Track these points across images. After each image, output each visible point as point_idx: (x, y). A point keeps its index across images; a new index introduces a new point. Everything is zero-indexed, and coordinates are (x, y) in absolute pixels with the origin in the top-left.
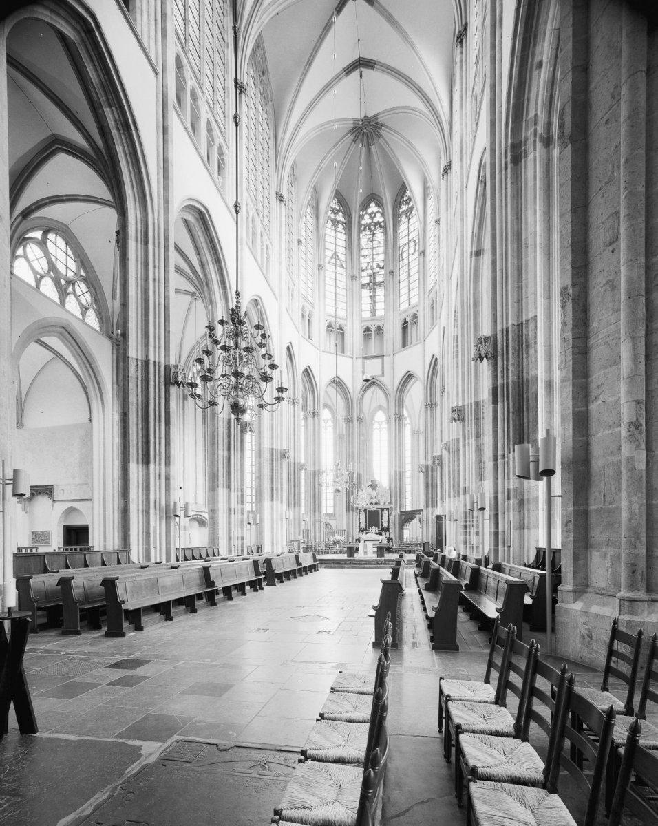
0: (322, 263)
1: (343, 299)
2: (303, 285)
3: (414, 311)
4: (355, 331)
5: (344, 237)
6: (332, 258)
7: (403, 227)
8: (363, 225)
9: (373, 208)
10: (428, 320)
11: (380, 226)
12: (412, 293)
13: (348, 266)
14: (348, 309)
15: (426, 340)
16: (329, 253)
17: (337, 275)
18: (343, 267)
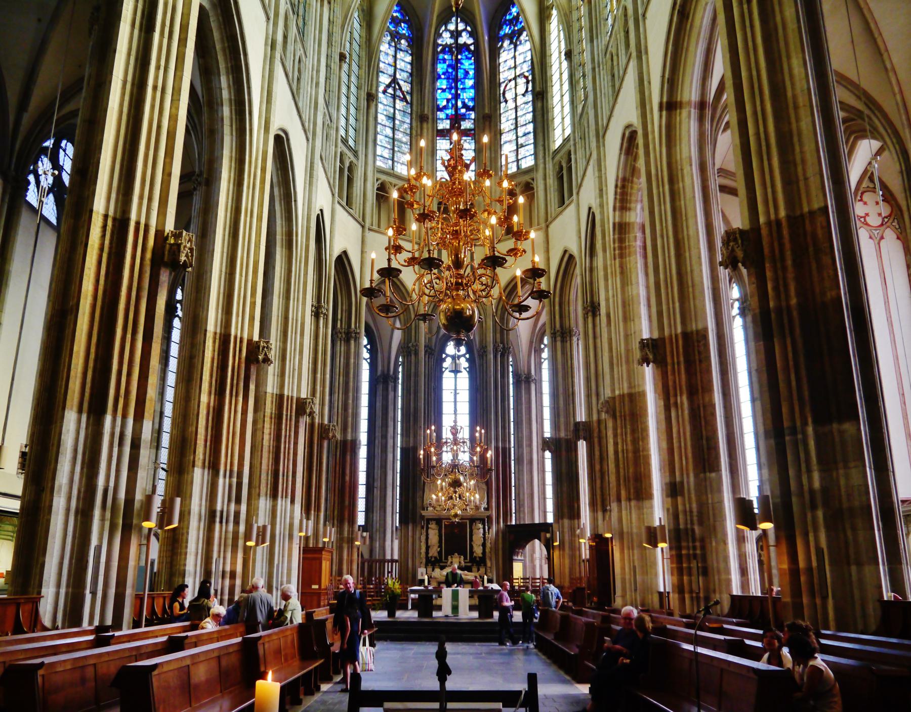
0: (374, 92)
1: (406, 148)
2: (343, 122)
3: (527, 178)
5: (409, 59)
6: (388, 86)
7: (505, 57)
8: (441, 45)
10: (553, 196)
11: (469, 51)
15: (552, 227)
16: (385, 80)
17: (397, 112)
18: (407, 101)
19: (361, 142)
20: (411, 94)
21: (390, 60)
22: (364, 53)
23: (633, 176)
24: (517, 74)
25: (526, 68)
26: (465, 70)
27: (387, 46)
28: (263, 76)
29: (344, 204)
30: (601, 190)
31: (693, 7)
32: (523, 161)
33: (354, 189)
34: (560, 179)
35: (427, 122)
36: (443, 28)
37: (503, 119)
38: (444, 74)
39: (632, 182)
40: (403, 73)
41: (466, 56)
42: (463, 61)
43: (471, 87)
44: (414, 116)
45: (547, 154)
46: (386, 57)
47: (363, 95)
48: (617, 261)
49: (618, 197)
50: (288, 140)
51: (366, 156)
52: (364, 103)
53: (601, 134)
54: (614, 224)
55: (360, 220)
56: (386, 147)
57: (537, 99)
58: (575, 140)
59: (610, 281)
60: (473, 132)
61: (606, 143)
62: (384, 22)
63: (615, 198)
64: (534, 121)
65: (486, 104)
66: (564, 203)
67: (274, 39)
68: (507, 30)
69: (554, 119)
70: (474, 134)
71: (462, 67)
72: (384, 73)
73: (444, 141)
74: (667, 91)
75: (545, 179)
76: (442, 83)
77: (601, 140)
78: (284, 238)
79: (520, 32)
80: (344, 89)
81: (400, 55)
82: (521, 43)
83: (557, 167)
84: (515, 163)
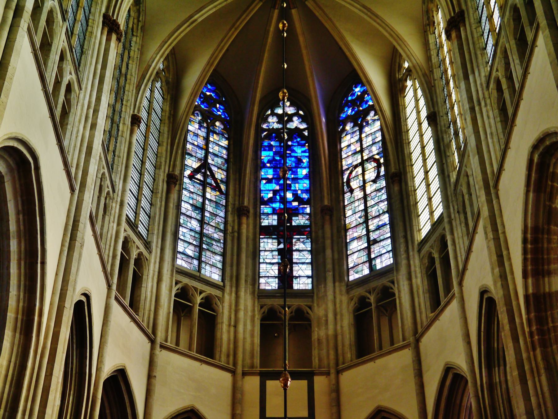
0: (177, 172)
1: (218, 247)
2: (130, 200)
3: (384, 281)
4: (241, 314)
5: (224, 143)
6: (196, 171)
8: (265, 130)
11: (303, 137)
12: (376, 249)
13: (231, 192)
14: (228, 269)
15: (425, 341)
16: (192, 163)
17: (207, 202)
19: (156, 232)
20: (227, 183)
21: (201, 142)
22: (166, 129)
23: (549, 224)
24: (365, 158)
25: (375, 150)
26: (296, 157)
27: (197, 126)
29: (127, 303)
30: (500, 257)
32: (378, 261)
33: (143, 290)
34: (431, 276)
35: (248, 217)
36: (269, 112)
37: (349, 213)
38: (269, 162)
39: (549, 232)
40: (216, 159)
41: (297, 142)
42: (295, 148)
43: (306, 177)
44: (230, 209)
45: (410, 247)
46: (195, 138)
47: (162, 176)
48: (538, 351)
49: (529, 256)
50: (37, 168)
51: (162, 250)
52: (162, 186)
53: (491, 184)
54: (526, 297)
55: (150, 331)
56: (190, 243)
57: (393, 182)
58: (449, 216)
59: (530, 383)
60: (308, 229)
61: (501, 193)
62: (193, 95)
63: (525, 260)
64: (390, 211)
65: (326, 194)
66: (439, 303)
69: (417, 203)
70: (310, 232)
71: (293, 154)
72: (192, 156)
73: (270, 241)
75: (410, 279)
76: (270, 173)
77: (492, 191)
78: (20, 317)
79: (366, 112)
80: (134, 161)
81: (214, 138)
83: (426, 261)
84: (367, 264)
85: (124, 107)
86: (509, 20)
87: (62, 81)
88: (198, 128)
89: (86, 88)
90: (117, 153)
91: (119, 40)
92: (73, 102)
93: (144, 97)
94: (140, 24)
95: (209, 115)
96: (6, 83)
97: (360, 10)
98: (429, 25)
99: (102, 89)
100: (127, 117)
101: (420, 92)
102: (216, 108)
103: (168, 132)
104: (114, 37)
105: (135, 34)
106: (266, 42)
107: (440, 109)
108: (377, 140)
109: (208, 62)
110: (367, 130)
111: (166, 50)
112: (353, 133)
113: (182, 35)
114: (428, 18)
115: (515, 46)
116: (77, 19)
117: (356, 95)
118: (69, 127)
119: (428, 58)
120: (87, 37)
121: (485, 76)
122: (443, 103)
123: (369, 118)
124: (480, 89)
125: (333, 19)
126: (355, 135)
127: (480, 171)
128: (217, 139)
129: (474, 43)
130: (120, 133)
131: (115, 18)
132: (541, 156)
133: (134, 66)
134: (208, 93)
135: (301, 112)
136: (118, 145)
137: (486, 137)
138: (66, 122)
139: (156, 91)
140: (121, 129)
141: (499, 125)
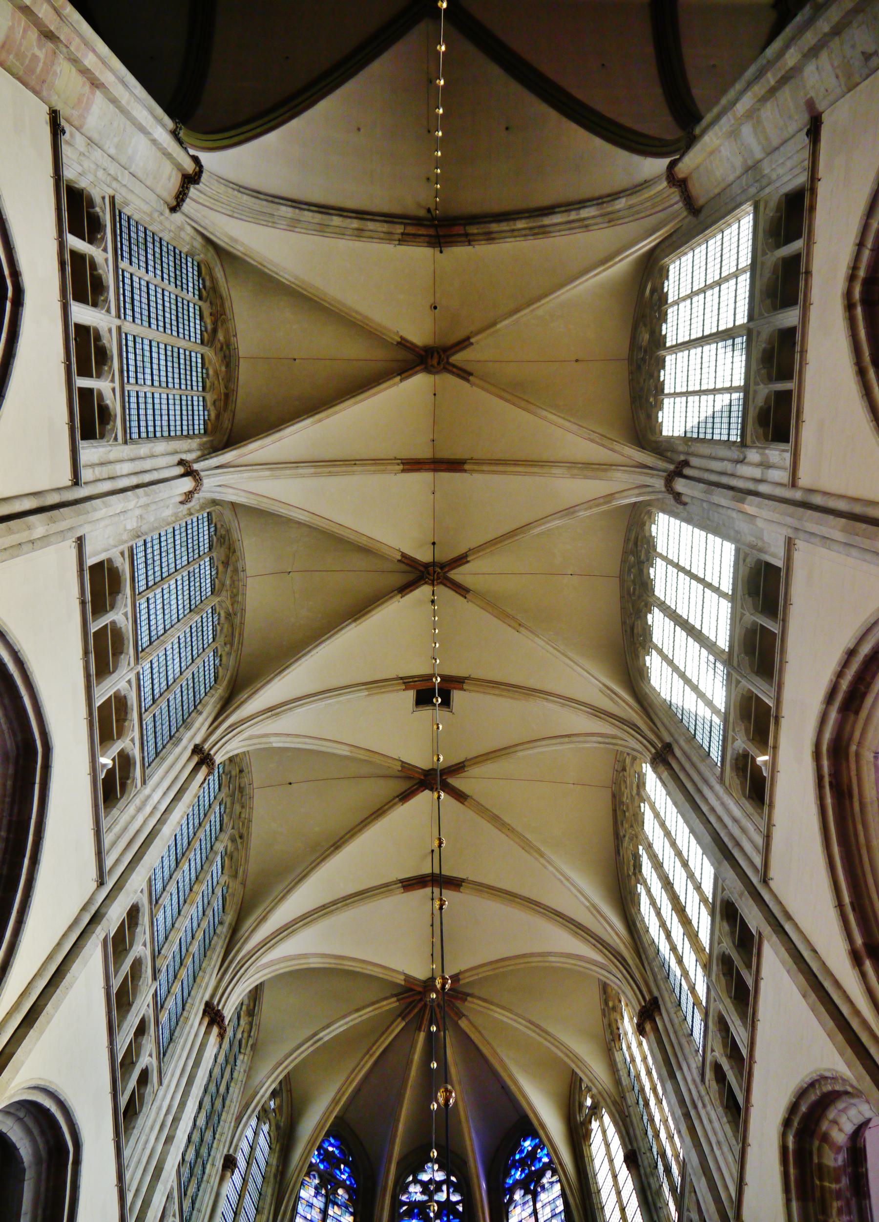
8: (405, 1203)
9: (432, 1173)
22: (270, 1191)
27: (312, 1191)
28: (59, 944)
31: (853, 773)
36: (411, 1178)
46: (308, 1209)
50: (77, 1162)
67: (103, 911)
68: (518, 1176)
74: (858, 925)
79: (541, 1173)
82: (543, 1188)
85: (216, 1142)
86: (717, 976)
87: (137, 1061)
88: (313, 1194)
89: (168, 1086)
90: (197, 1206)
91: (221, 1036)
92: (148, 1098)
93: (244, 1136)
94: (251, 1042)
95: (329, 1177)
96: (58, 991)
97: (526, 1027)
98: (613, 1040)
99: (189, 1092)
100: (218, 1156)
101: (611, 1130)
102: (340, 1170)
103: (273, 1195)
104: (215, 1030)
105: (242, 1051)
106: (409, 1075)
107: (641, 1144)
108: (557, 1211)
109: (334, 1099)
110: (543, 1197)
111: (280, 1074)
112: (524, 1204)
113: (303, 1056)
114: (612, 1033)
115: (731, 1005)
116: (172, 991)
117: (525, 1151)
118: (136, 1132)
119: (618, 1082)
120: (180, 1023)
121: (697, 1067)
122: (643, 1136)
123: (545, 1181)
124: (692, 1087)
125: (493, 1044)
126: (527, 1206)
127: (711, 1198)
128: (339, 1213)
129: (675, 1032)
130: (205, 1178)
131: (220, 1007)
132: (799, 1136)
133: (237, 1091)
134: (330, 1149)
135: (453, 1179)
136: (200, 1193)
137: (712, 1150)
138: (132, 1125)
139: (262, 1135)
140: (207, 1171)
141: (727, 1128)
